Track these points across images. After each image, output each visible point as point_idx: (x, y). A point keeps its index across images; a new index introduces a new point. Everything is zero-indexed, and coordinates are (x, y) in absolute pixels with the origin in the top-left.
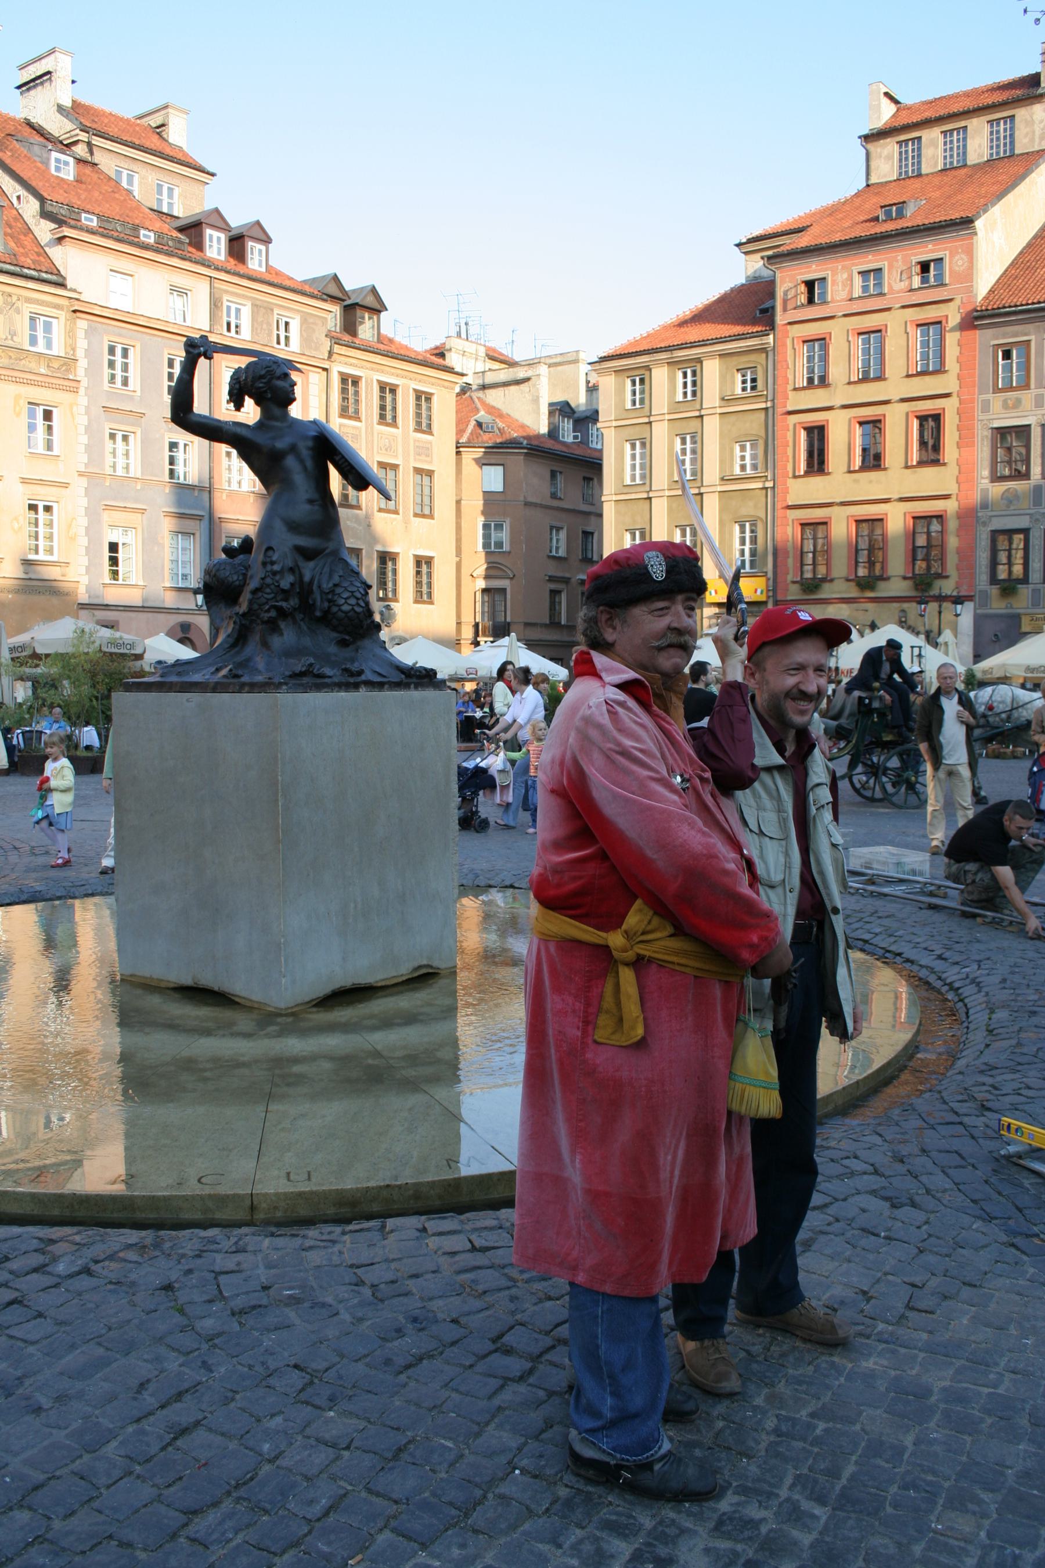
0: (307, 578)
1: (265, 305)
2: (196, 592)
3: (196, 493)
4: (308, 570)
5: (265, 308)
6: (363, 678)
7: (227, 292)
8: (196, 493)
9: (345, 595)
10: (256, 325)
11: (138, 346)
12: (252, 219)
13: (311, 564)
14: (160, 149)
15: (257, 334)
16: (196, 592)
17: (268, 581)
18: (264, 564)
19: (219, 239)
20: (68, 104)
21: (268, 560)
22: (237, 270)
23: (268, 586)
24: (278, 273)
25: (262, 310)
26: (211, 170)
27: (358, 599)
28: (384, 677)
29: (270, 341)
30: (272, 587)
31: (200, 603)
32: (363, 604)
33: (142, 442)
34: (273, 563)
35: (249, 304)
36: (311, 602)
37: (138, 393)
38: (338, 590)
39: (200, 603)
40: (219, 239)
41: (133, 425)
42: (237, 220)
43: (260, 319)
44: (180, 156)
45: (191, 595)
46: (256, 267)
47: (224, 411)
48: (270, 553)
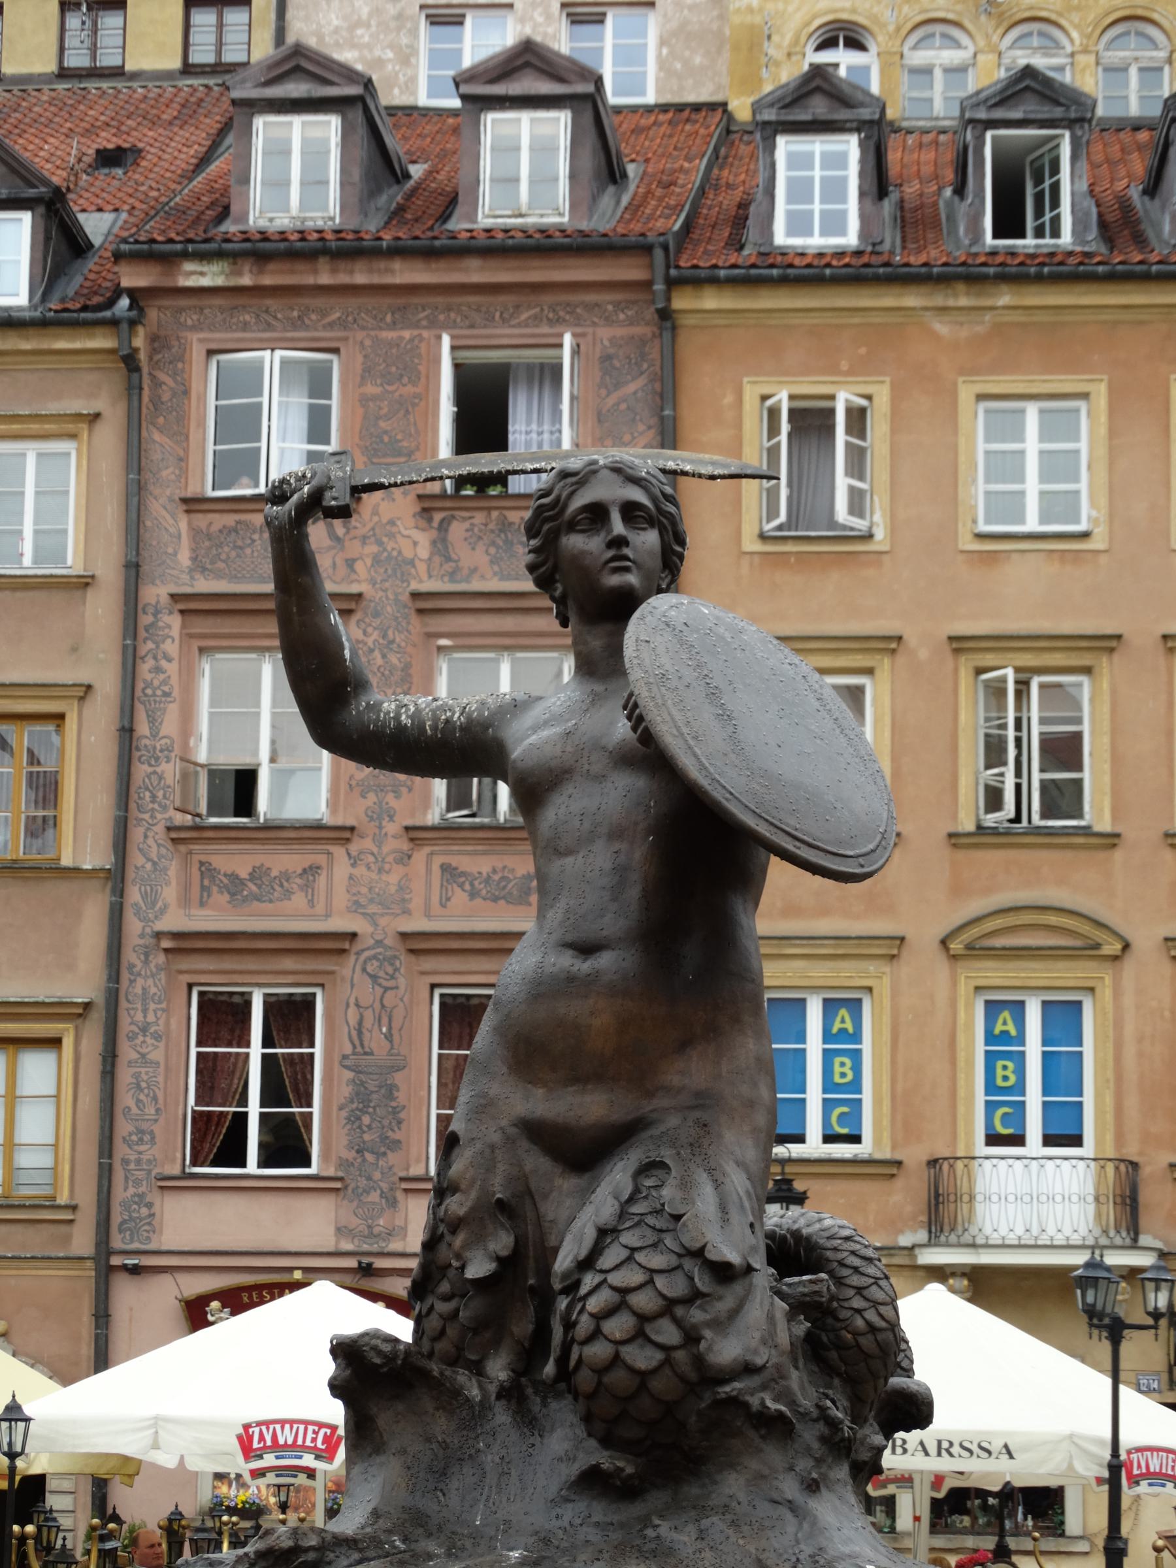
9: (594, 1304)
27: (643, 1318)
30: (451, 1273)
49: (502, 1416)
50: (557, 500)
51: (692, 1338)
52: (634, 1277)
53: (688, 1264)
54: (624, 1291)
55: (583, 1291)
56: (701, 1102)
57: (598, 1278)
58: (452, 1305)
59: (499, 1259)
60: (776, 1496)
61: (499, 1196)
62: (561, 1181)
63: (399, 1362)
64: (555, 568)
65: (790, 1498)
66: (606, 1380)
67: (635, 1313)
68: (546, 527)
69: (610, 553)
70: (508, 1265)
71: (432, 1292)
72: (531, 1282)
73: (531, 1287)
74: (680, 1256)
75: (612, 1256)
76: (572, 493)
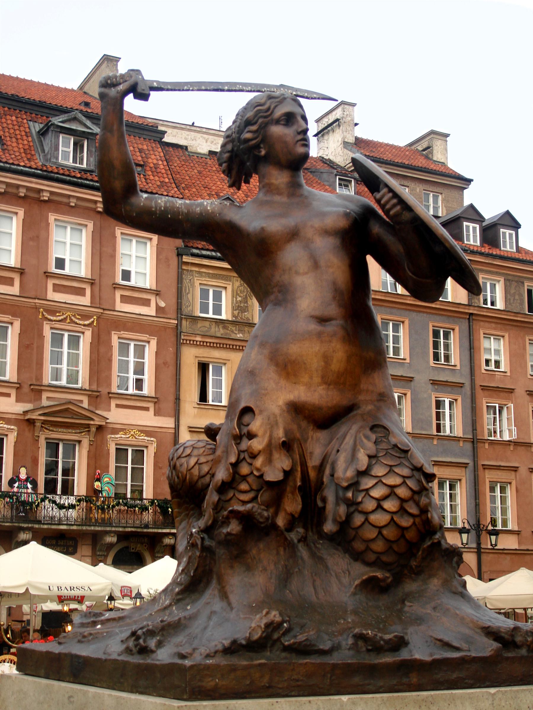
0: (313, 462)
1: (516, 279)
2: (461, 531)
3: (461, 444)
4: (316, 445)
5: (517, 282)
6: (404, 655)
7: (482, 271)
8: (461, 444)
9: (377, 493)
10: (509, 297)
11: (407, 322)
12: (501, 210)
13: (322, 435)
14: (425, 165)
15: (510, 304)
16: (461, 531)
17: (245, 469)
18: (238, 438)
19: (474, 229)
20: (352, 140)
21: (245, 430)
22: (491, 252)
23: (244, 478)
24: (527, 252)
25: (514, 284)
26: (467, 176)
27: (403, 501)
28: (457, 649)
29: (523, 309)
30: (250, 479)
31: (465, 541)
32: (414, 510)
33: (412, 401)
34: (251, 436)
35: (502, 280)
36: (320, 504)
37: (408, 361)
38: (367, 483)
39: (465, 541)
40: (475, 229)
41: (403, 387)
42: (489, 213)
43: (513, 291)
44: (442, 169)
45: (458, 535)
46: (508, 249)
47: (484, 372)
48: (246, 419)
49: (303, 552)
50: (268, 109)
51: (424, 511)
52: (398, 481)
53: (416, 474)
54: (392, 487)
55: (363, 487)
56: (382, 398)
57: (374, 481)
58: (251, 495)
59: (285, 472)
60: (454, 589)
61: (284, 439)
62: (312, 432)
63: (270, 521)
64: (263, 141)
65: (461, 591)
66: (385, 532)
67: (399, 498)
68: (260, 121)
69: (300, 137)
70: (287, 474)
71: (234, 488)
72: (299, 484)
73: (300, 486)
74: (412, 470)
75: (379, 471)
76: (276, 106)
